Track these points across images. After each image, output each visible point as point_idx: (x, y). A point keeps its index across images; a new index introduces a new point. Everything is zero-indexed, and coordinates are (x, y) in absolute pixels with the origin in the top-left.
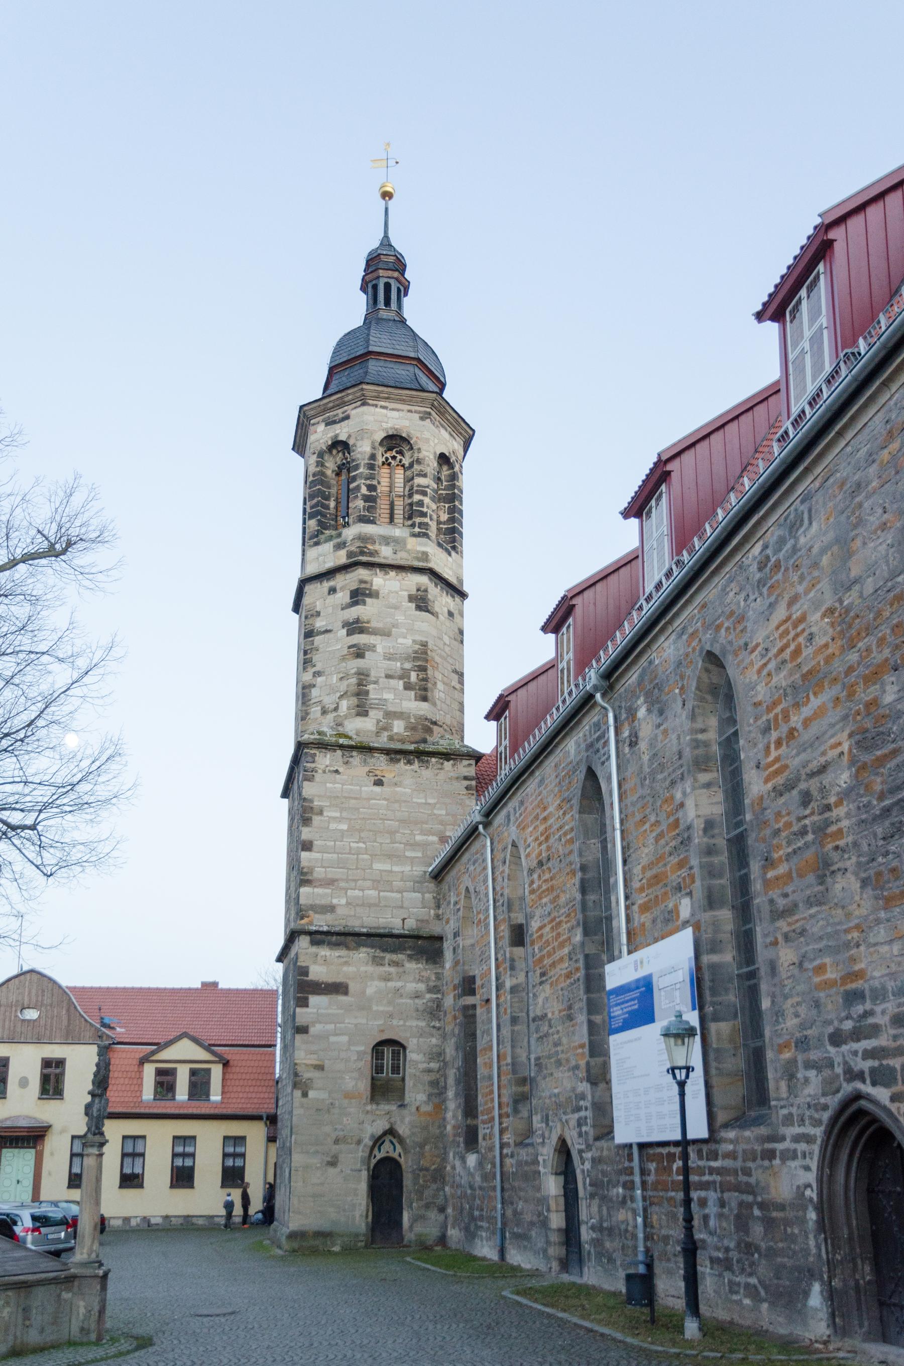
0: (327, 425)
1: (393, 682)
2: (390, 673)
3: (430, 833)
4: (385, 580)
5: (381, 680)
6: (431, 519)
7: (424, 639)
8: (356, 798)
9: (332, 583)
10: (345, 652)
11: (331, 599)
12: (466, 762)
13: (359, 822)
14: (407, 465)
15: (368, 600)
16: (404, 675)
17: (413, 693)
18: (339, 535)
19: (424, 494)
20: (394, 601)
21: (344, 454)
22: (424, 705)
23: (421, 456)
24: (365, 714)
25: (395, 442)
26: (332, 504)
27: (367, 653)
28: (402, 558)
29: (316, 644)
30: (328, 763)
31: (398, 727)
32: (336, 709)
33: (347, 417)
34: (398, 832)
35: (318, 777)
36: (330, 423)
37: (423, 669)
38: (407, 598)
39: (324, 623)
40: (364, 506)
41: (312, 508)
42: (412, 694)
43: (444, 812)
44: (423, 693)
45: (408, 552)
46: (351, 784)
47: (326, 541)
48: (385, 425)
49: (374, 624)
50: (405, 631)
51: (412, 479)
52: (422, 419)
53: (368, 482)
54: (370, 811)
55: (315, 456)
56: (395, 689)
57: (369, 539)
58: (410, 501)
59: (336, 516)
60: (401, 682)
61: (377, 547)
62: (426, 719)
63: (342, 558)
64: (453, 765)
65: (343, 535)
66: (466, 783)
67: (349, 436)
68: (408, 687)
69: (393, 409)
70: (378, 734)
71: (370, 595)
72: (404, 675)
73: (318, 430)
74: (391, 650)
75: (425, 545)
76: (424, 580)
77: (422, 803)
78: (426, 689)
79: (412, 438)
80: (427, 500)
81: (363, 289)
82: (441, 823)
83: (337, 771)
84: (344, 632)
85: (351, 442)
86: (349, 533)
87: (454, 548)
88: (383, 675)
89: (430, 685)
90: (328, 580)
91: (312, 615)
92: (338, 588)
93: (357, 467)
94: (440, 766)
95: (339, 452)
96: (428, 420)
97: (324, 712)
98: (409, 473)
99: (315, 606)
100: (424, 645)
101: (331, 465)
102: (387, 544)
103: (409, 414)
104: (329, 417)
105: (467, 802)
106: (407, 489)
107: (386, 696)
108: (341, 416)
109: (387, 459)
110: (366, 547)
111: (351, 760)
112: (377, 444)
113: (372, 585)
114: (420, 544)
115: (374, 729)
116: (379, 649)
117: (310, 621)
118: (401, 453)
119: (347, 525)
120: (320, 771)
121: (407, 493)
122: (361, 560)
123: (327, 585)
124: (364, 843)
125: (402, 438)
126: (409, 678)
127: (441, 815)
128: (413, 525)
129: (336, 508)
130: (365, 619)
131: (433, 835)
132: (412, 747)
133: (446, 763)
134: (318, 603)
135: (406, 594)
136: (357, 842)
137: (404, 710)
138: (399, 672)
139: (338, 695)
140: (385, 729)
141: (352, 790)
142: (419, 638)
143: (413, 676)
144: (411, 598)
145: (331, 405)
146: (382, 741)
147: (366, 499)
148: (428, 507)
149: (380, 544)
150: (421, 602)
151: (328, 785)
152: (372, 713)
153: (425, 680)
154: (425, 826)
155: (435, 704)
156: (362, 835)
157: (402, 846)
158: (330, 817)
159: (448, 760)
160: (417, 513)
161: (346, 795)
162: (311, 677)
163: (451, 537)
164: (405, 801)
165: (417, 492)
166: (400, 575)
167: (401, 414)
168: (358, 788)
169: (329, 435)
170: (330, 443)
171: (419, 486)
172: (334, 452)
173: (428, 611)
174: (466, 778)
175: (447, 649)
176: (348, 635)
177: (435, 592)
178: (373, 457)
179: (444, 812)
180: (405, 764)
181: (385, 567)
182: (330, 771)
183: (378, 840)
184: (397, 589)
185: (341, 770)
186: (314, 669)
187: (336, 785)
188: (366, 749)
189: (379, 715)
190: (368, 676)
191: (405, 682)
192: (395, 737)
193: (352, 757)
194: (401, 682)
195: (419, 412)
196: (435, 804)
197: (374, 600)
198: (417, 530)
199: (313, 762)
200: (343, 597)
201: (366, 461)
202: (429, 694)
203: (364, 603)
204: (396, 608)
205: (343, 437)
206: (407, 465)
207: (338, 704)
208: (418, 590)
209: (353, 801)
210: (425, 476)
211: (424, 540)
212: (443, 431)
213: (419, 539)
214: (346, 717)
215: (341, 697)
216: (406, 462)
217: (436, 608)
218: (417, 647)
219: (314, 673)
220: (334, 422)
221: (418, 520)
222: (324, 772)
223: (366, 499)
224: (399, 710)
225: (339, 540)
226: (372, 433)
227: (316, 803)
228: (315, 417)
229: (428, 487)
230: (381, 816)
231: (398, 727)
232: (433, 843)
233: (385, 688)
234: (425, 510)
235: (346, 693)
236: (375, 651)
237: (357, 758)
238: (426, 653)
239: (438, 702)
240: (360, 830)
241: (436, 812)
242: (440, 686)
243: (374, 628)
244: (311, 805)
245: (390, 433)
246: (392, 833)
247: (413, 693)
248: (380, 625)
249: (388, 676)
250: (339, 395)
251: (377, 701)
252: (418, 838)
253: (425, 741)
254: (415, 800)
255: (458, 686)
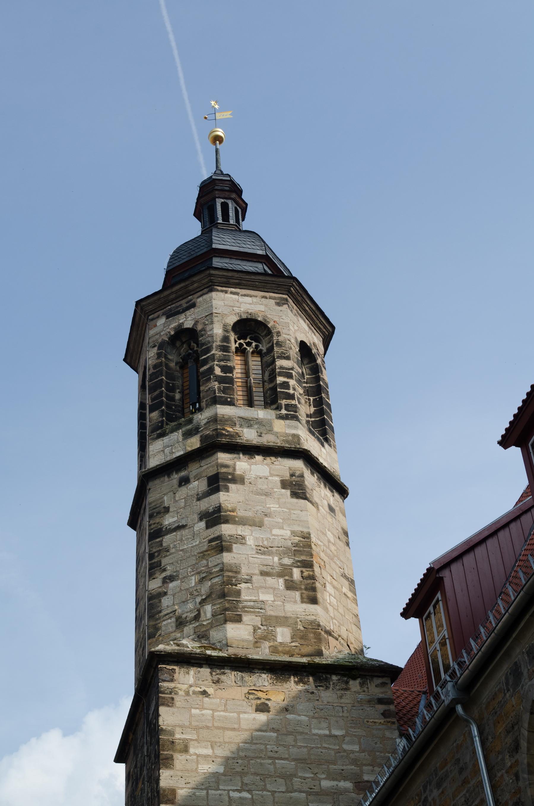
0: (167, 318)
1: (270, 581)
2: (265, 569)
3: (342, 776)
4: (250, 465)
5: (255, 578)
6: (299, 403)
7: (305, 530)
8: (234, 729)
9: (183, 474)
10: (205, 548)
11: (183, 491)
12: (379, 681)
13: (240, 761)
14: (264, 349)
15: (232, 486)
16: (284, 572)
17: (297, 594)
18: (190, 421)
19: (290, 376)
20: (264, 487)
21: (189, 345)
22: (311, 608)
23: (281, 339)
24: (238, 619)
25: (250, 329)
26: (178, 396)
27: (234, 546)
28: (268, 440)
29: (164, 544)
30: (191, 681)
31: (283, 635)
32: (197, 618)
33: (193, 305)
34: (295, 776)
35: (179, 700)
36: (170, 315)
37: (308, 565)
38: (279, 484)
39: (176, 519)
40: (219, 388)
41: (153, 400)
42: (297, 595)
43: (356, 748)
44: (311, 593)
45: (276, 434)
46: (225, 710)
47: (172, 431)
48: (237, 310)
49: (241, 513)
50: (281, 521)
51: (274, 362)
52: (278, 304)
53: (222, 363)
54: (254, 747)
55: (156, 348)
56: (274, 589)
57: (227, 420)
58: (271, 385)
59: (183, 409)
60: (281, 581)
61: (238, 429)
62: (319, 625)
63: (194, 443)
64: (362, 685)
65: (195, 421)
66: (382, 708)
67: (196, 323)
68: (290, 586)
69: (245, 295)
70: (256, 643)
71: (234, 480)
72: (284, 572)
73: (158, 324)
74: (266, 543)
75: (296, 428)
76: (298, 465)
77: (326, 736)
78: (314, 589)
79: (269, 322)
80: (292, 382)
81: (198, 214)
82: (354, 762)
83: (204, 693)
84: (202, 524)
85: (199, 327)
86: (202, 418)
87: (327, 440)
88: (257, 572)
89: (318, 585)
90: (178, 471)
91: (159, 513)
92: (191, 476)
93: (209, 350)
94: (344, 686)
95: (183, 343)
96: (286, 306)
97: (181, 623)
98: (268, 358)
99: (163, 502)
100: (307, 537)
101: (174, 360)
102: (250, 426)
103: (263, 299)
104: (170, 310)
105: (388, 734)
106: (267, 374)
107: (263, 597)
108: (185, 306)
109: (241, 344)
110: (224, 429)
111: (223, 677)
112: (230, 328)
113: (234, 469)
114: (289, 427)
115: (251, 638)
116: (250, 541)
117: (157, 520)
118: (257, 340)
119: (200, 410)
120: (181, 693)
121: (266, 378)
122: (218, 442)
123: (176, 477)
124: (249, 791)
125: (256, 321)
126: (291, 575)
127: (353, 752)
128: (279, 408)
129: (182, 399)
130: (230, 507)
131: (345, 779)
132: (304, 660)
133: (351, 682)
134: (165, 498)
135: (278, 479)
136: (239, 791)
137: (289, 614)
138: (278, 569)
139: (198, 599)
140: (265, 638)
141: (226, 718)
142: (298, 528)
143: (296, 573)
144: (284, 484)
145: (173, 296)
146: (263, 653)
147: (221, 380)
148: (294, 389)
149: (241, 426)
150: (298, 490)
151: (194, 711)
152: (246, 618)
153: (313, 577)
154: (332, 767)
155: (326, 610)
156: (246, 780)
157: (304, 795)
158: (198, 756)
159: (354, 679)
160: (283, 396)
161: (220, 725)
162: (160, 584)
163: (322, 428)
164: (302, 733)
165: (281, 374)
166: (268, 458)
167: (255, 299)
168: (235, 715)
169: (172, 326)
170: (172, 333)
171: (281, 367)
172: (178, 344)
173: (306, 498)
174: (380, 701)
175: (333, 548)
176: (208, 527)
177: (311, 480)
178: (226, 339)
179: (356, 748)
180: (297, 683)
181: (250, 450)
182: (194, 693)
183: (269, 787)
184: (267, 474)
185: (210, 691)
186: (164, 575)
187: (204, 712)
188: (244, 665)
189: (257, 621)
190: (237, 572)
191: (286, 580)
192: (280, 649)
193: (224, 673)
194: (281, 581)
195: (274, 298)
196: (344, 736)
197: (239, 486)
198: (284, 412)
199: (172, 680)
200: (199, 485)
201: (219, 343)
202: (319, 596)
203: (227, 489)
204: (267, 494)
205: (188, 324)
206: (264, 349)
207: (199, 611)
208: (292, 475)
209: (229, 733)
210: (288, 358)
211: (293, 423)
212: (301, 321)
213: (288, 422)
214: (211, 626)
215: (203, 602)
216: (263, 348)
217: (316, 499)
218: (297, 539)
219: (165, 578)
220: (179, 313)
221: (284, 402)
222: (187, 693)
223: (221, 380)
224: (282, 614)
225: (189, 427)
226: (224, 315)
227: (178, 736)
228: (153, 312)
229: (292, 369)
230: (271, 754)
231: (283, 635)
232: (346, 790)
233: (261, 587)
234: (291, 391)
235: (209, 596)
236: (245, 544)
237: (231, 677)
238: (310, 546)
239: (330, 609)
240: (242, 774)
241: (345, 747)
242: (329, 587)
243: (242, 518)
244: (171, 738)
245: (244, 316)
246: (287, 777)
247: (297, 594)
248: (249, 514)
249: (264, 574)
250: (182, 285)
251: (252, 603)
252: (326, 784)
253: (320, 653)
254: (315, 731)
255: (350, 594)
